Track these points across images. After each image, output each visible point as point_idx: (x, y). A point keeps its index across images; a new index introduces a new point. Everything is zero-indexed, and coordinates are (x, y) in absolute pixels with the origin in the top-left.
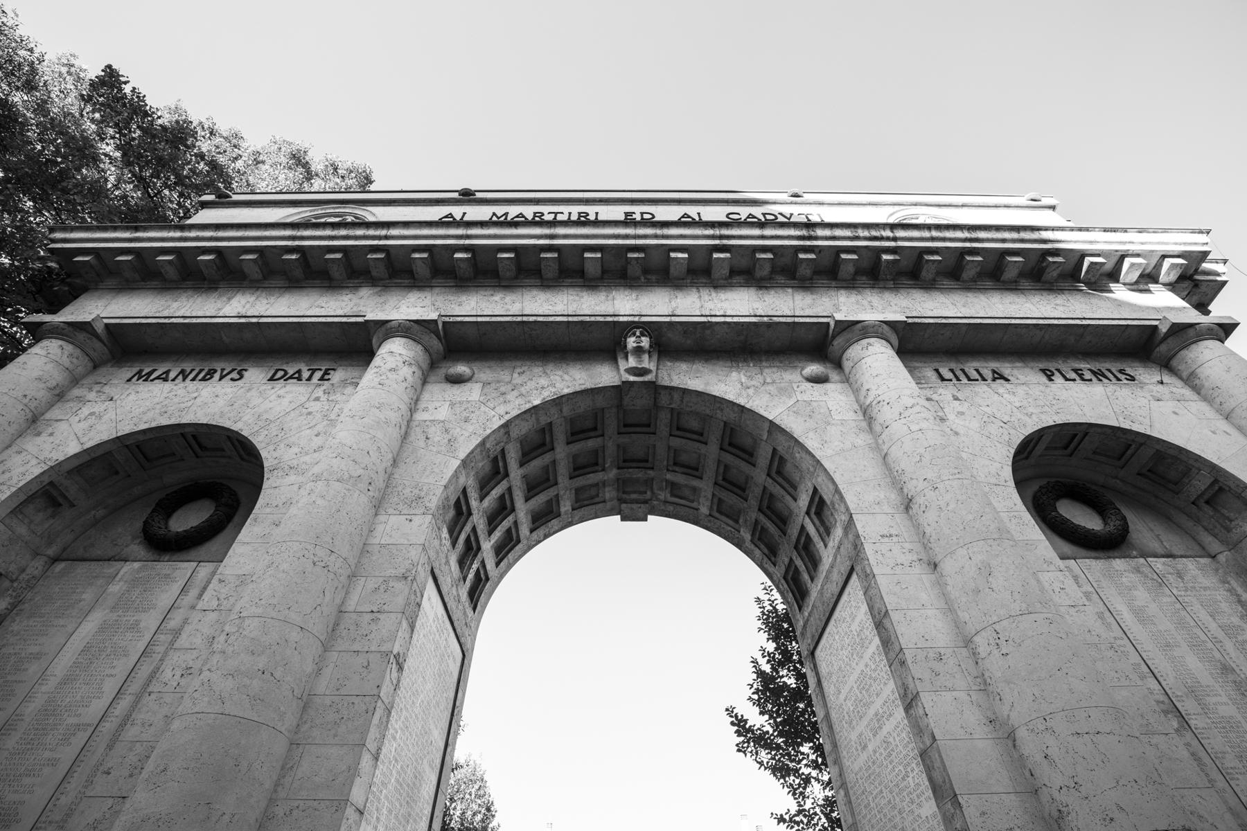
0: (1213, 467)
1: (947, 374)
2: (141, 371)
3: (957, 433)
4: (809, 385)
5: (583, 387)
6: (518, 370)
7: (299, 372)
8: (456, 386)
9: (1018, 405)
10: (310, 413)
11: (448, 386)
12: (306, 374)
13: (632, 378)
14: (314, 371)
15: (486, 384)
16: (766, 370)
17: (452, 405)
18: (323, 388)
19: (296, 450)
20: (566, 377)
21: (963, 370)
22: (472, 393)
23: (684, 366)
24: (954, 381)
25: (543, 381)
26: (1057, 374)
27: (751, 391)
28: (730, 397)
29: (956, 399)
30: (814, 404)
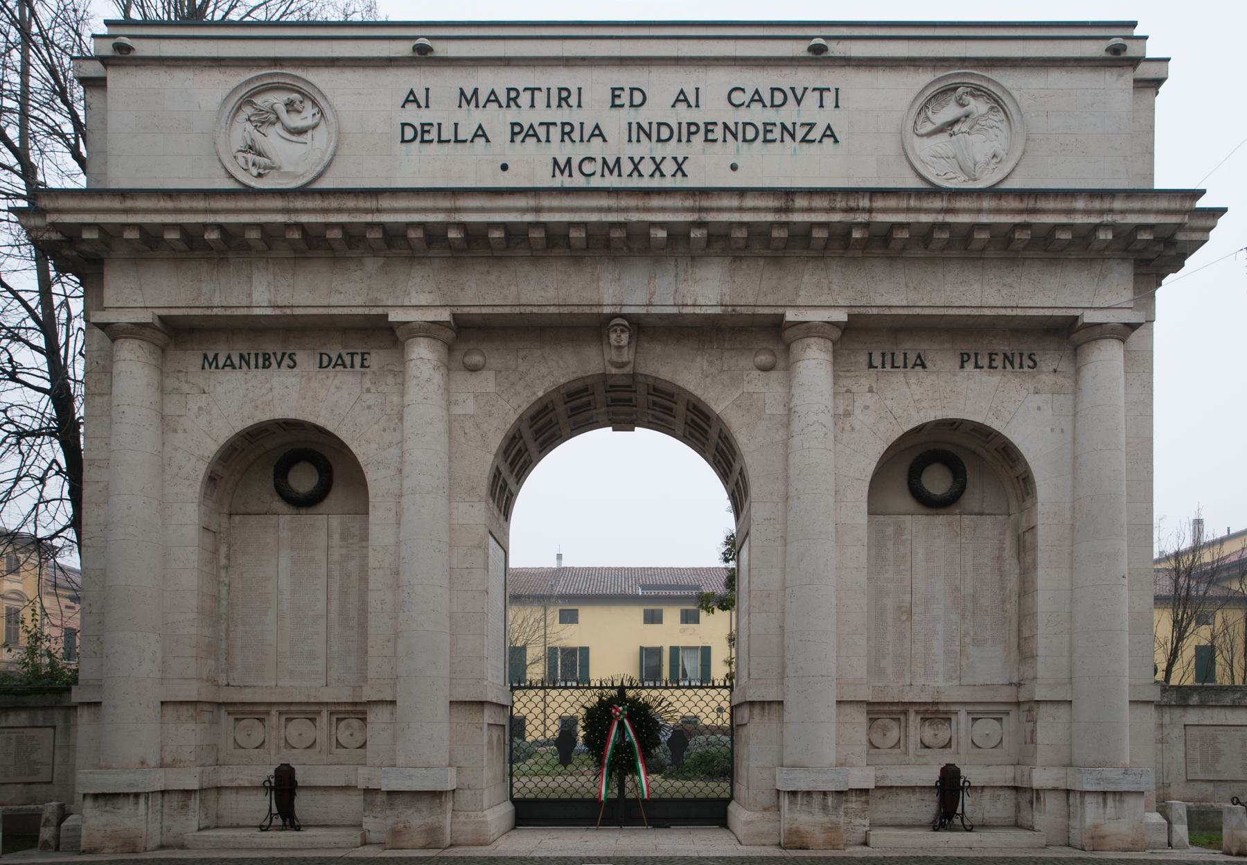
0: (1026, 464)
1: (877, 360)
2: (206, 357)
3: (853, 429)
4: (757, 373)
5: (575, 376)
6: (521, 354)
7: (340, 356)
8: (474, 374)
9: (916, 397)
10: (369, 407)
11: (467, 374)
12: (348, 360)
13: (614, 371)
14: (352, 355)
15: (498, 372)
16: (726, 354)
17: (476, 397)
18: (368, 377)
19: (374, 446)
20: (561, 363)
21: (893, 354)
22: (486, 382)
23: (658, 348)
24: (880, 369)
25: (544, 370)
26: (973, 360)
27: (708, 380)
28: (691, 388)
29: (871, 391)
30: (755, 396)
